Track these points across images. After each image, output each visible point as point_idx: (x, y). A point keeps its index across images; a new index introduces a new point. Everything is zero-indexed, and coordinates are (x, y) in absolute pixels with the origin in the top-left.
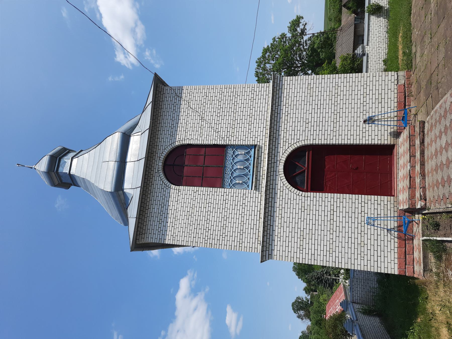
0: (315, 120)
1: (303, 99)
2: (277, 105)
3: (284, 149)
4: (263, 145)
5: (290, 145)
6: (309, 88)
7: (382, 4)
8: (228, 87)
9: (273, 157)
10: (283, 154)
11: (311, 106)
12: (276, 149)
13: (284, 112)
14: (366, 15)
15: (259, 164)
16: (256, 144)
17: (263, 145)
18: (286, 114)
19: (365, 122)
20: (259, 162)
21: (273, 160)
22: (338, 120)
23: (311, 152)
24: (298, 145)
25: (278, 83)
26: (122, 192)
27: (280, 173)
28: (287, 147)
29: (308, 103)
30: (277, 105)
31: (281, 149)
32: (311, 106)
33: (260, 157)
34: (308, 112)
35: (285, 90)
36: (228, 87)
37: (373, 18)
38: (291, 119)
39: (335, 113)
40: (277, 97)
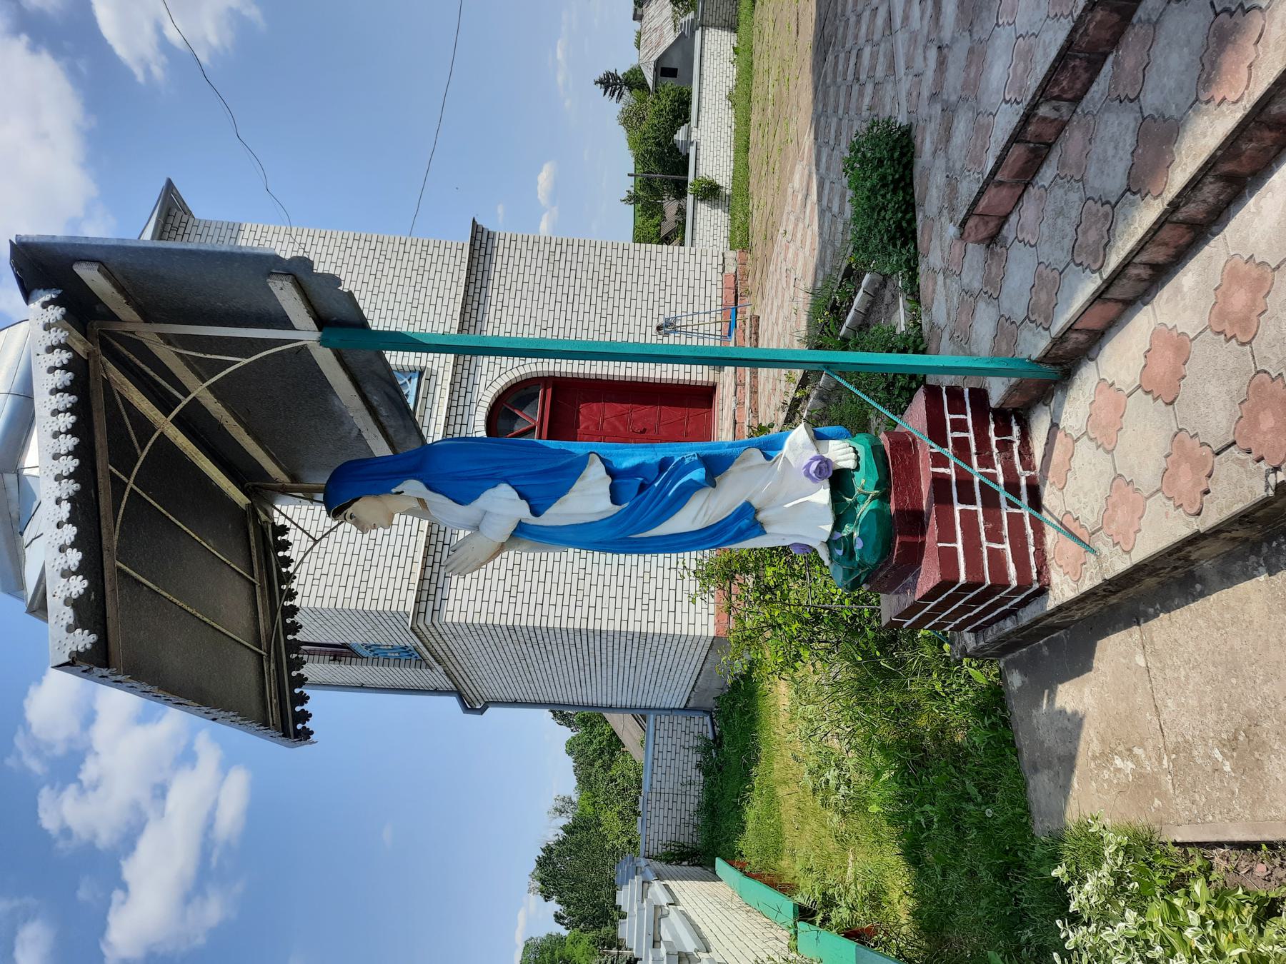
0: (562, 325)
1: (537, 281)
2: (478, 285)
3: (490, 377)
4: (441, 370)
5: (503, 371)
6: (551, 260)
7: (720, 182)
8: (363, 236)
9: (462, 393)
10: (486, 389)
11: (553, 296)
12: (471, 377)
13: (494, 302)
14: (690, 198)
15: (428, 411)
16: (423, 365)
17: (441, 370)
18: (499, 307)
19: (659, 328)
20: (429, 405)
21: (462, 400)
22: (608, 329)
23: (549, 391)
24: (523, 372)
25: (484, 241)
26: (15, 476)
27: (477, 429)
28: (496, 375)
29: (548, 290)
30: (478, 285)
31: (483, 378)
32: (553, 296)
33: (430, 396)
34: (546, 307)
35: (499, 258)
36: (363, 236)
37: (702, 208)
38: (510, 318)
39: (604, 314)
40: (480, 268)
